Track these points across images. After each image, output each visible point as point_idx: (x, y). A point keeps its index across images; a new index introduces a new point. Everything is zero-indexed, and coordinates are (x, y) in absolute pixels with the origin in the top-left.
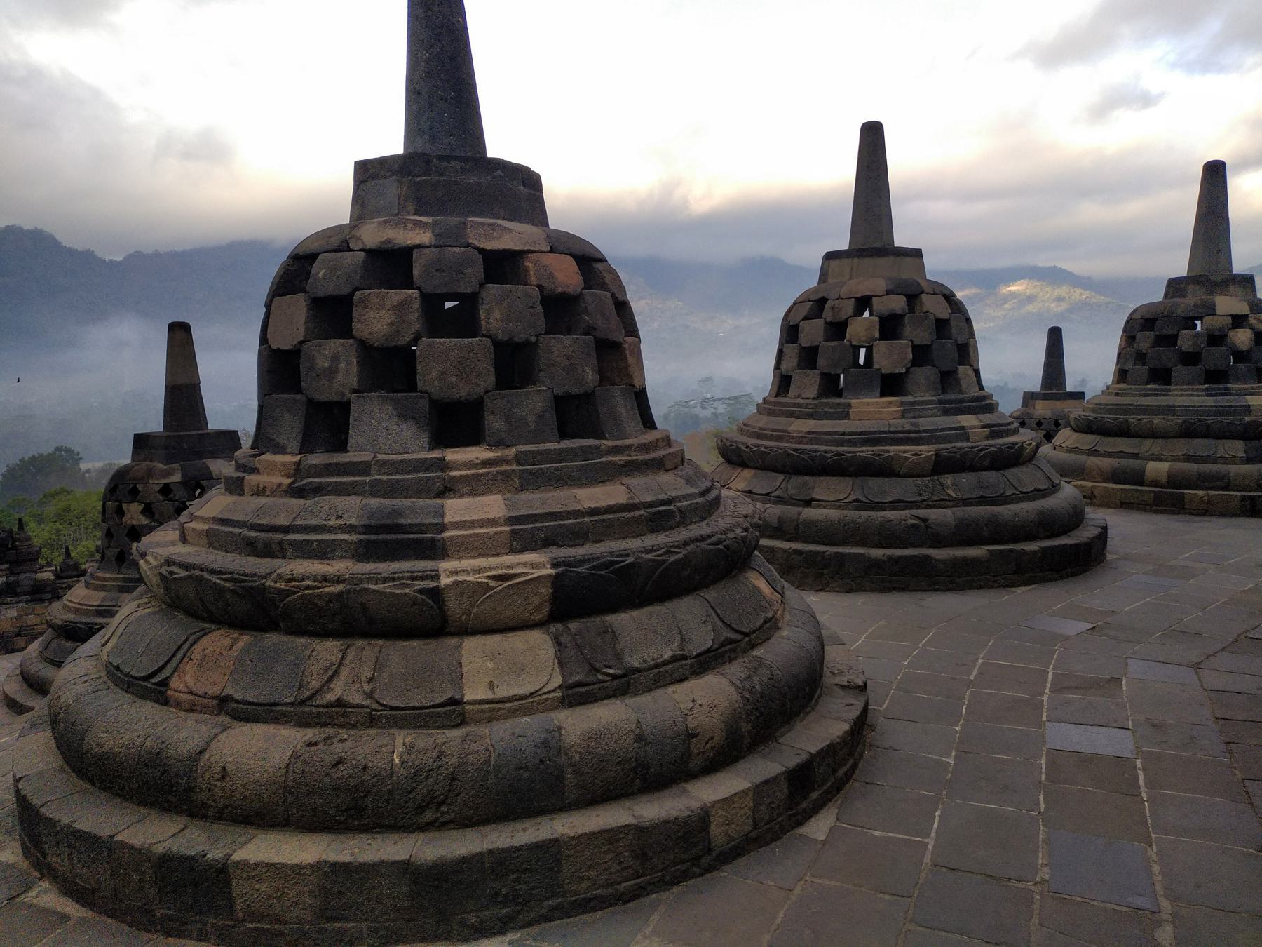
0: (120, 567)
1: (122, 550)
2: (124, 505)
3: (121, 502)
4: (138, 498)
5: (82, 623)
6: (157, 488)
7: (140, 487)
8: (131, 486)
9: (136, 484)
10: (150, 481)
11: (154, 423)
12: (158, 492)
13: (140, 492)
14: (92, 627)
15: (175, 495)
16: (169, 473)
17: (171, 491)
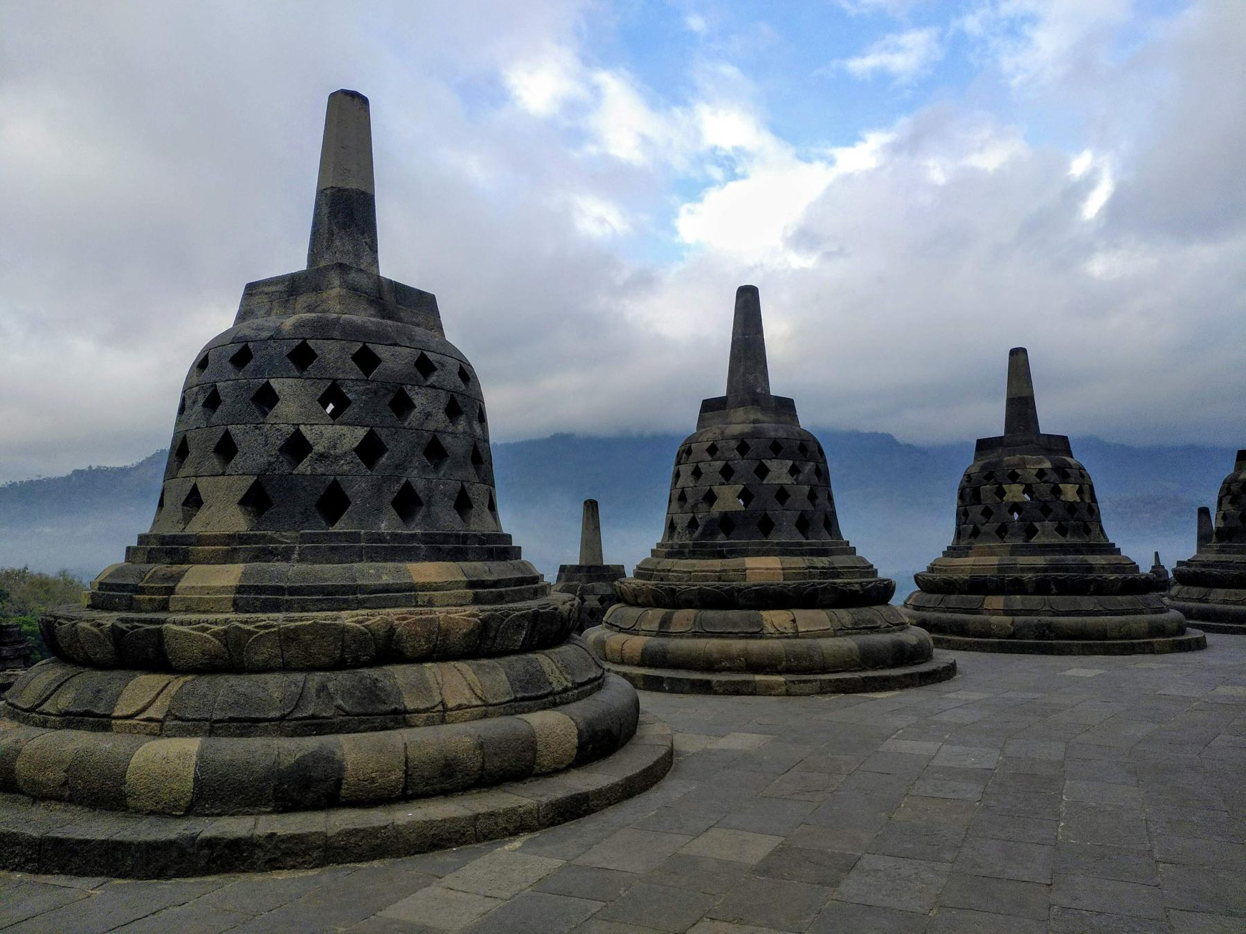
0: (1002, 537)
1: (1003, 524)
2: (1004, 486)
3: (1000, 485)
4: (1018, 480)
5: (992, 576)
6: (1035, 472)
7: (1019, 471)
8: (1010, 471)
9: (1014, 470)
10: (1027, 467)
11: (997, 428)
12: (1036, 476)
13: (1019, 475)
14: (1003, 580)
15: (1050, 478)
16: (1040, 462)
17: (1045, 474)
